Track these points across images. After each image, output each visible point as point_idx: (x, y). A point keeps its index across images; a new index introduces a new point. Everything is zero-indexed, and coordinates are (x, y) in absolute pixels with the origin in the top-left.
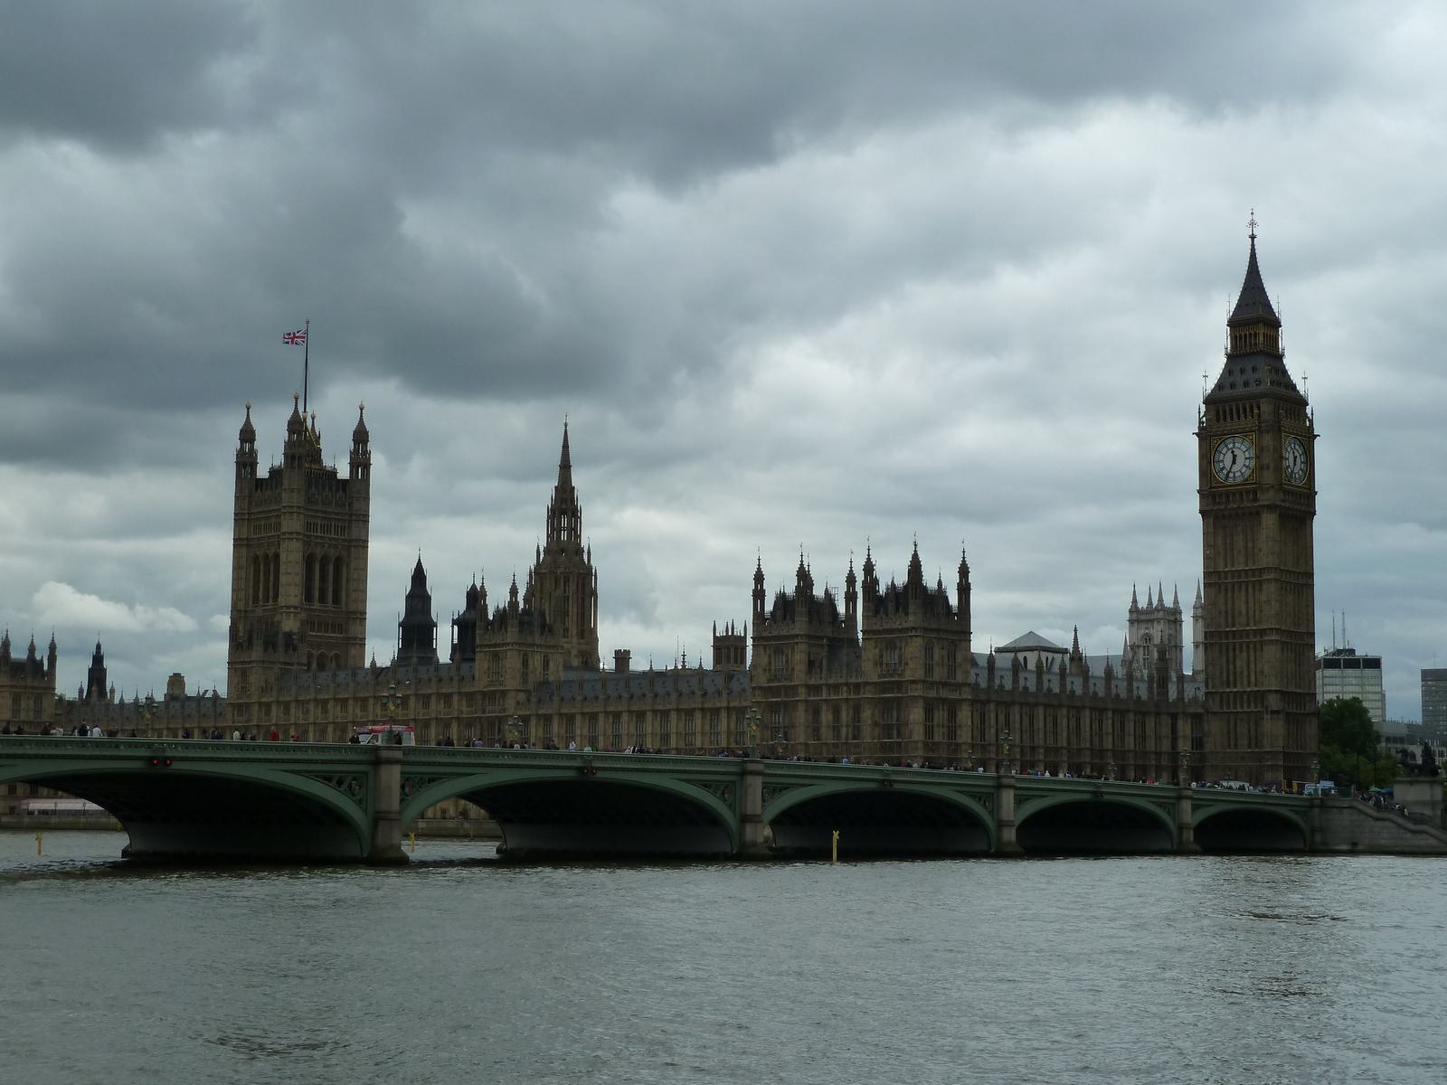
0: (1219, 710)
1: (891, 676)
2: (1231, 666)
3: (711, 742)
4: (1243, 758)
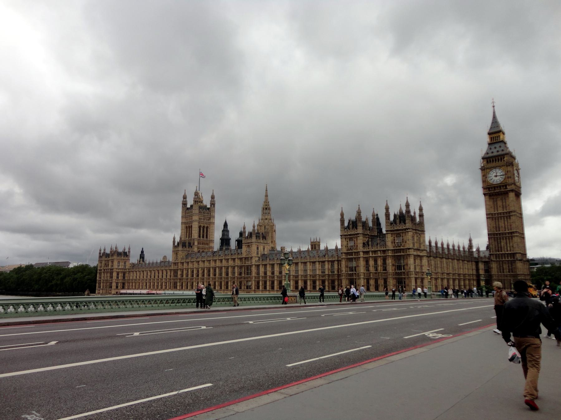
0: (495, 260)
1: (400, 247)
2: (499, 245)
3: (322, 272)
4: (507, 276)
